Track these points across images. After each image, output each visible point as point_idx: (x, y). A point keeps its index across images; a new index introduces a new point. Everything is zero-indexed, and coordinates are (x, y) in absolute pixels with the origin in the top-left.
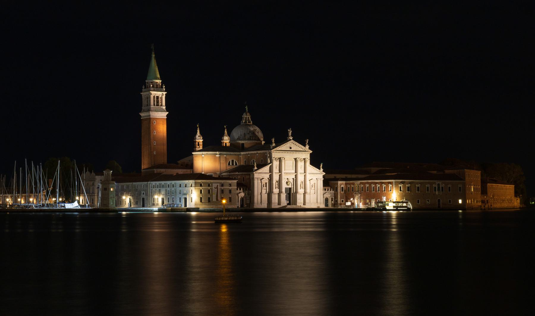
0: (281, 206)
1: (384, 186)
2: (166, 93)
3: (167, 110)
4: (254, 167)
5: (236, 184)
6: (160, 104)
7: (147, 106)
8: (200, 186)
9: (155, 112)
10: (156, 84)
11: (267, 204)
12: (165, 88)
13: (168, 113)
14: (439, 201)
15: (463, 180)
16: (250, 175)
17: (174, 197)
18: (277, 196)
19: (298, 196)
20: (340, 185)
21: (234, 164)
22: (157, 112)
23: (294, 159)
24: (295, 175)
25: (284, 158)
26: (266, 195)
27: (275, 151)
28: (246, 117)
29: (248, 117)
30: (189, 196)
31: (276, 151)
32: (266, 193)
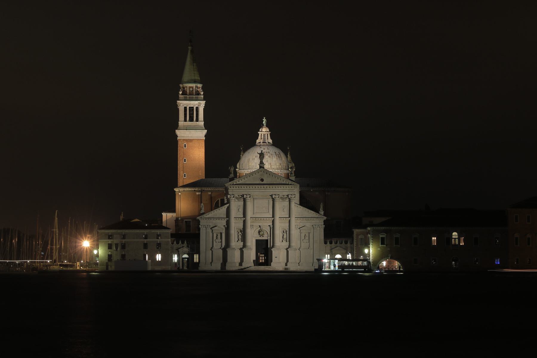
0: (242, 267)
3: (206, 126)
8: (108, 239)
9: (186, 130)
10: (189, 90)
11: (222, 264)
18: (237, 253)
19: (275, 252)
20: (358, 235)
22: (187, 130)
23: (270, 197)
24: (273, 222)
25: (249, 196)
26: (221, 251)
27: (233, 185)
29: (264, 135)
31: (235, 185)
32: (221, 248)
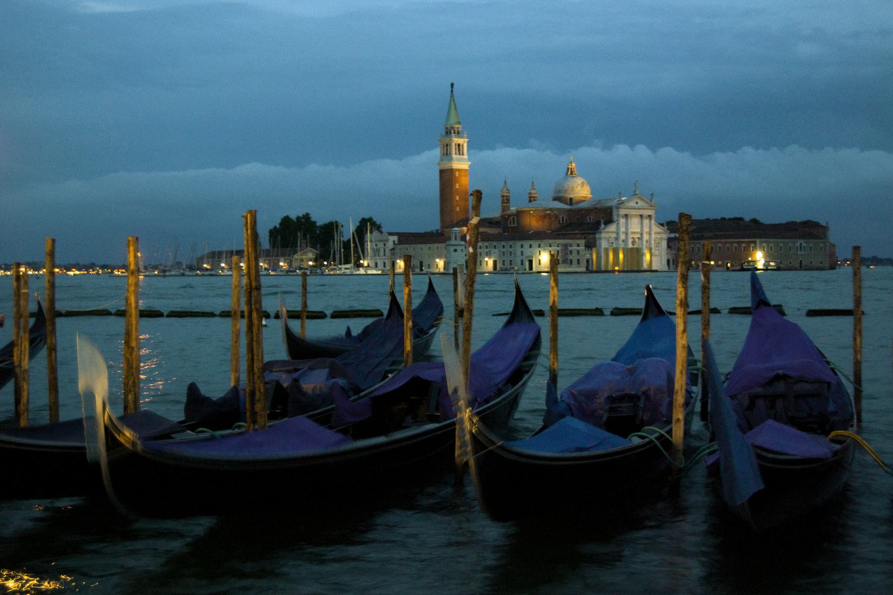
1: (744, 245)
2: (467, 140)
3: (469, 159)
4: (600, 225)
5: (583, 244)
6: (461, 153)
7: (447, 154)
12: (466, 134)
13: (470, 163)
14: (801, 261)
15: (821, 238)
16: (594, 234)
17: (512, 259)
21: (565, 222)
28: (571, 168)
30: (535, 258)
